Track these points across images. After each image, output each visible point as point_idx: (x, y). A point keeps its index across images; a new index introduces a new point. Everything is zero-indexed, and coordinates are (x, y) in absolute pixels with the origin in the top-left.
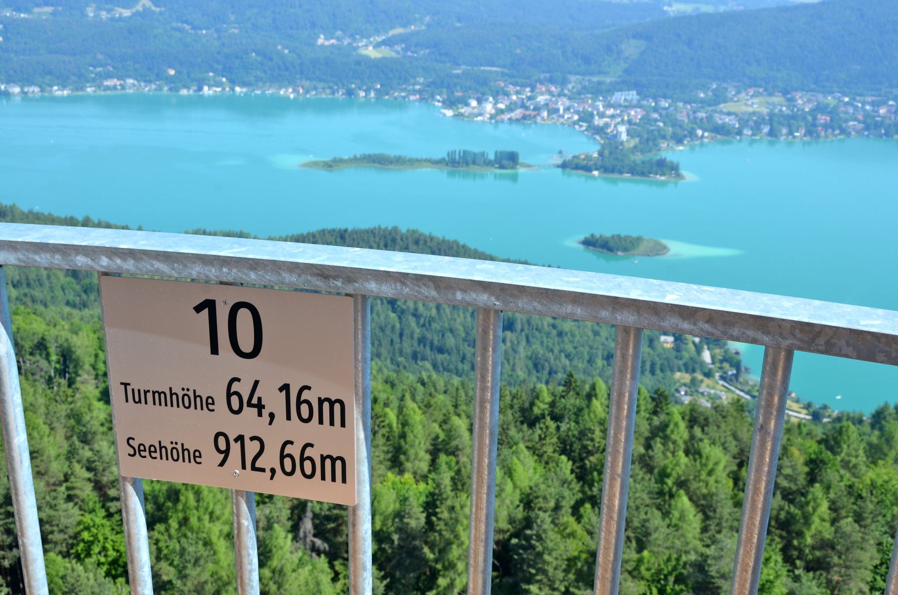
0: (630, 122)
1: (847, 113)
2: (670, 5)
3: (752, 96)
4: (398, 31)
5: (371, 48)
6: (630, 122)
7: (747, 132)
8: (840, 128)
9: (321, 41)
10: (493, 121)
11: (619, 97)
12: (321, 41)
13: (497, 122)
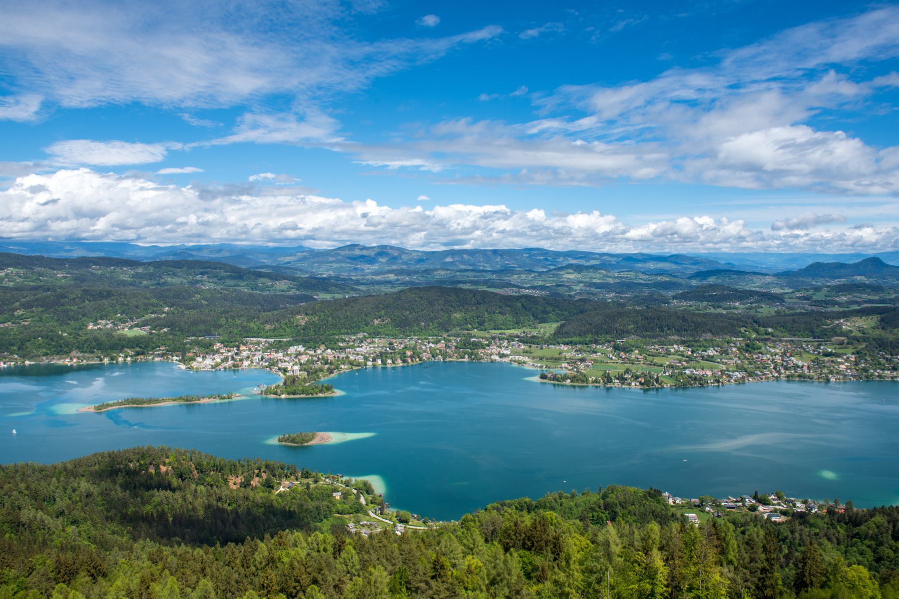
0: (301, 364)
1: (421, 348)
2: (318, 296)
3: (370, 343)
4: (147, 317)
5: (126, 329)
6: (301, 364)
7: (369, 363)
8: (419, 357)
9: (90, 327)
10: (213, 370)
11: (292, 350)
12: (90, 327)
13: (216, 371)
